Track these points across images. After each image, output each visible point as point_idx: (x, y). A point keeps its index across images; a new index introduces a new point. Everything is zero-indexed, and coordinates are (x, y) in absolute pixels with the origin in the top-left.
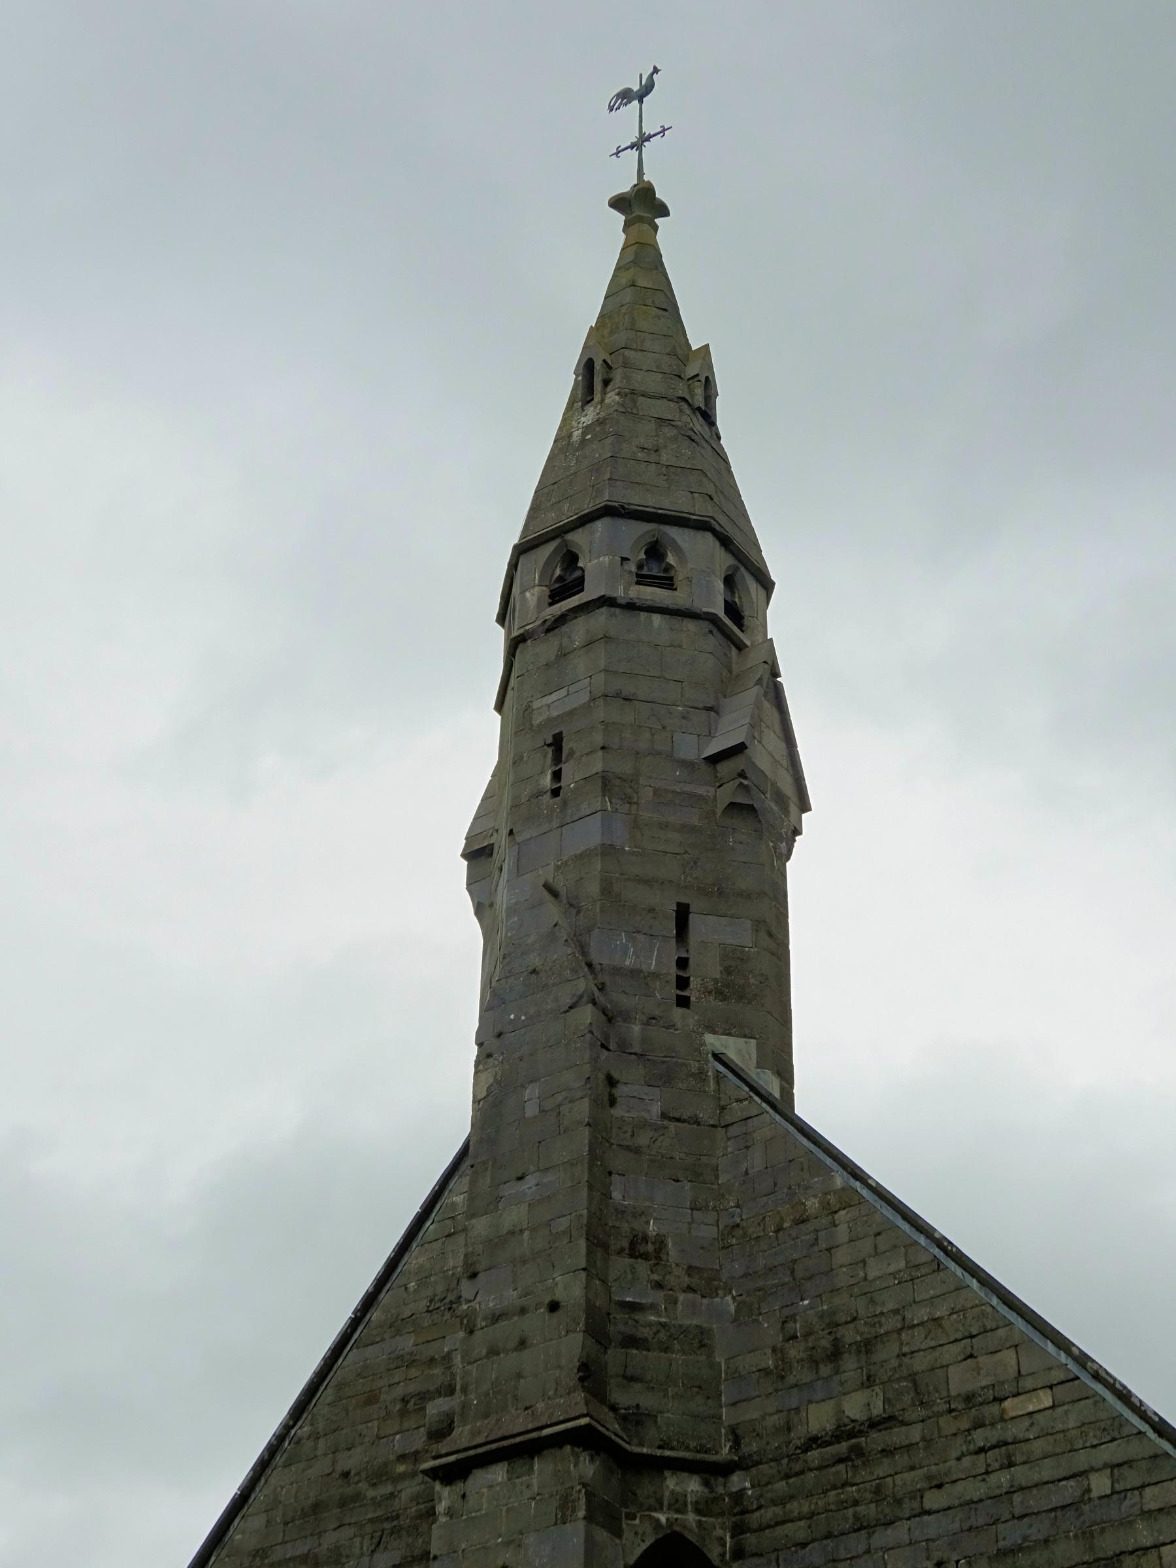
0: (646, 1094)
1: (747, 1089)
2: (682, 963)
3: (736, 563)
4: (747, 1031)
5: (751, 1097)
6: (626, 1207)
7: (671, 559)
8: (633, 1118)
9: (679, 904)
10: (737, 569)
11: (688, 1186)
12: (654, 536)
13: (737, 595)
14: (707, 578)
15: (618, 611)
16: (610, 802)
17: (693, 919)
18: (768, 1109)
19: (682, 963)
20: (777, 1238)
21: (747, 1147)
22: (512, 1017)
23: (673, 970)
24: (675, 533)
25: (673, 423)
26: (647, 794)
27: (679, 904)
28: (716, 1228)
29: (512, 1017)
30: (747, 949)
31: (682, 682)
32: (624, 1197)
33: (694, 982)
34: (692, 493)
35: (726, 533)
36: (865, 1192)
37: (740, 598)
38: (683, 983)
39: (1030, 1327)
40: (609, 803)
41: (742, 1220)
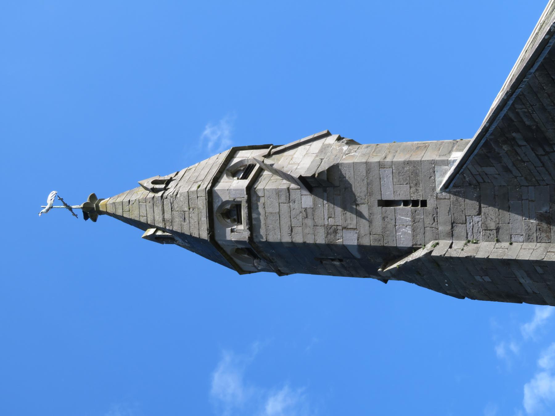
0: (470, 223)
1: (458, 175)
2: (406, 203)
3: (225, 172)
4: (431, 171)
5: (461, 173)
6: (526, 234)
7: (228, 207)
8: (483, 230)
9: (379, 206)
10: (228, 170)
11: (511, 202)
12: (219, 216)
13: (240, 168)
14: (232, 191)
15: (254, 235)
16: (339, 239)
17: (385, 198)
18: (465, 166)
19: (406, 203)
20: (527, 162)
21: (486, 174)
22: (447, 285)
23: (410, 207)
24: (216, 205)
25: (172, 202)
26: (331, 221)
27: (379, 206)
28: (529, 187)
29: (447, 285)
30: (394, 171)
31: (279, 203)
32: (521, 235)
33: (414, 198)
34: (198, 197)
35: (212, 181)
36: (493, 127)
37: (241, 167)
38: (415, 203)
39: (541, 55)
40: (339, 240)
41: (522, 176)
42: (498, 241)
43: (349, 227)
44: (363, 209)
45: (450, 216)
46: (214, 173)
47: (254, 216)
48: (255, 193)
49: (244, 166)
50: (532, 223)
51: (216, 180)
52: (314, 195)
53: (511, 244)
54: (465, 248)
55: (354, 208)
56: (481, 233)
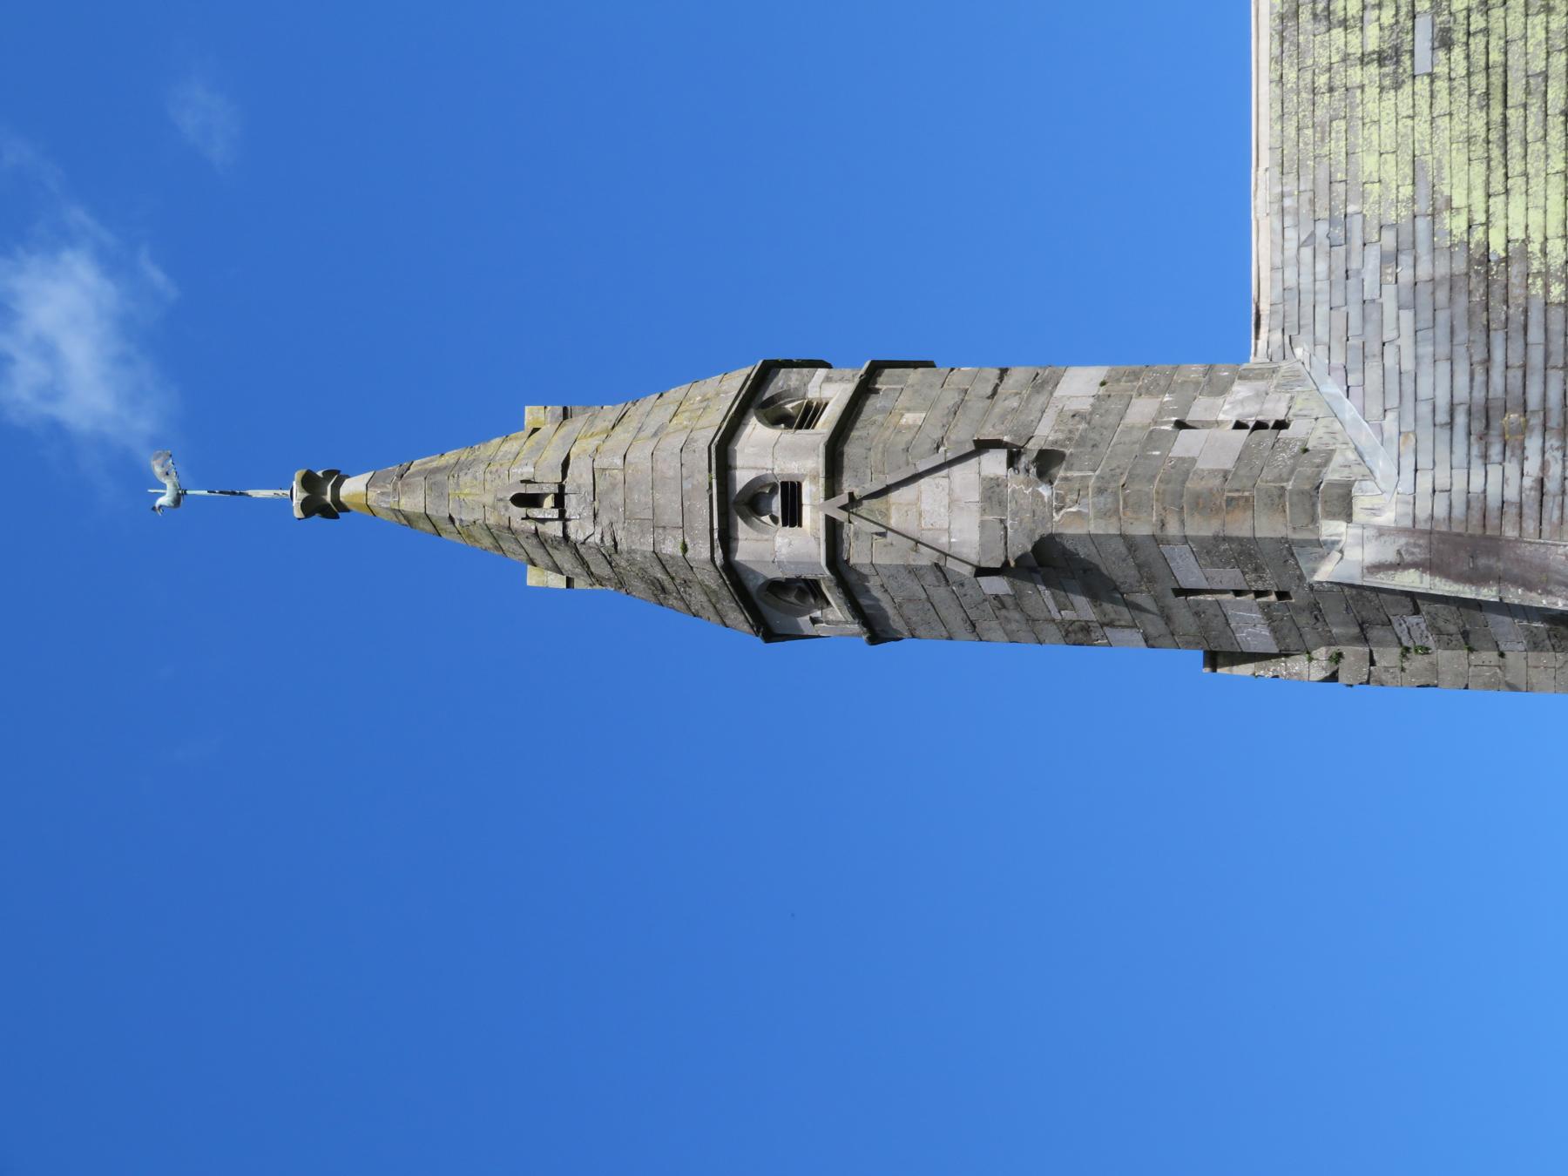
3: (733, 511)
12: (766, 595)
13: (760, 491)
42: (1471, 650)
43: (1117, 623)
44: (1142, 599)
45: (1352, 614)
46: (706, 512)
47: (864, 602)
48: (852, 569)
49: (769, 484)
50: (1536, 627)
51: (726, 539)
52: (1008, 576)
53: (1502, 655)
54: (1406, 665)
55: (1118, 598)
56: (1431, 638)
